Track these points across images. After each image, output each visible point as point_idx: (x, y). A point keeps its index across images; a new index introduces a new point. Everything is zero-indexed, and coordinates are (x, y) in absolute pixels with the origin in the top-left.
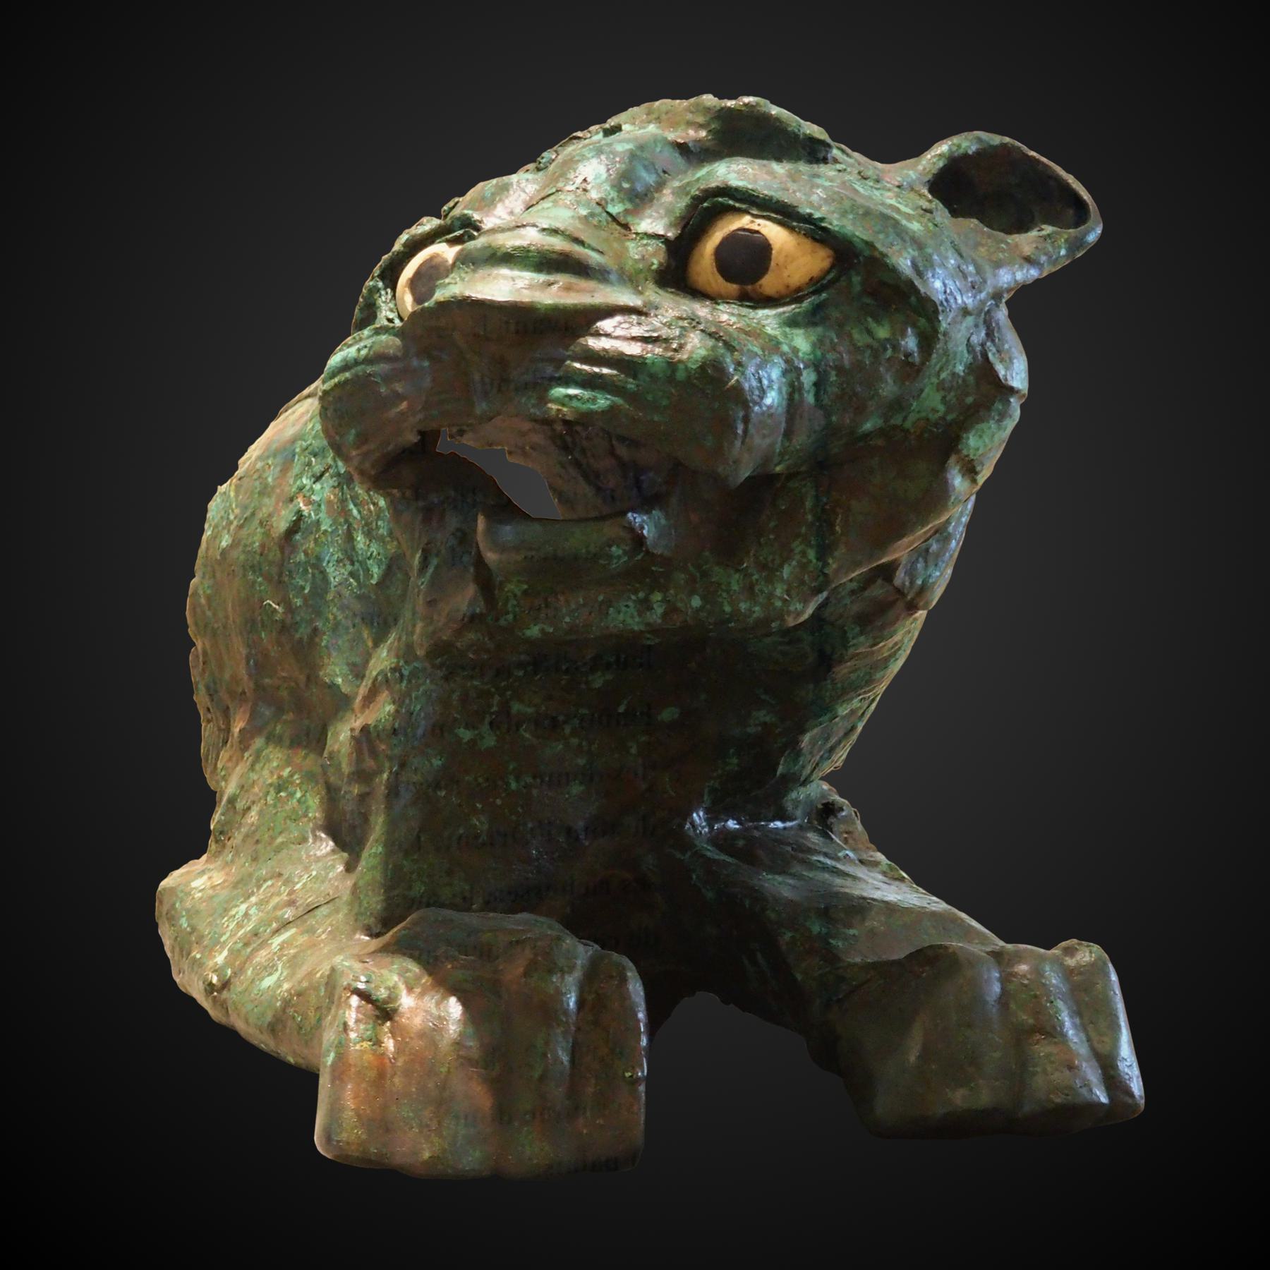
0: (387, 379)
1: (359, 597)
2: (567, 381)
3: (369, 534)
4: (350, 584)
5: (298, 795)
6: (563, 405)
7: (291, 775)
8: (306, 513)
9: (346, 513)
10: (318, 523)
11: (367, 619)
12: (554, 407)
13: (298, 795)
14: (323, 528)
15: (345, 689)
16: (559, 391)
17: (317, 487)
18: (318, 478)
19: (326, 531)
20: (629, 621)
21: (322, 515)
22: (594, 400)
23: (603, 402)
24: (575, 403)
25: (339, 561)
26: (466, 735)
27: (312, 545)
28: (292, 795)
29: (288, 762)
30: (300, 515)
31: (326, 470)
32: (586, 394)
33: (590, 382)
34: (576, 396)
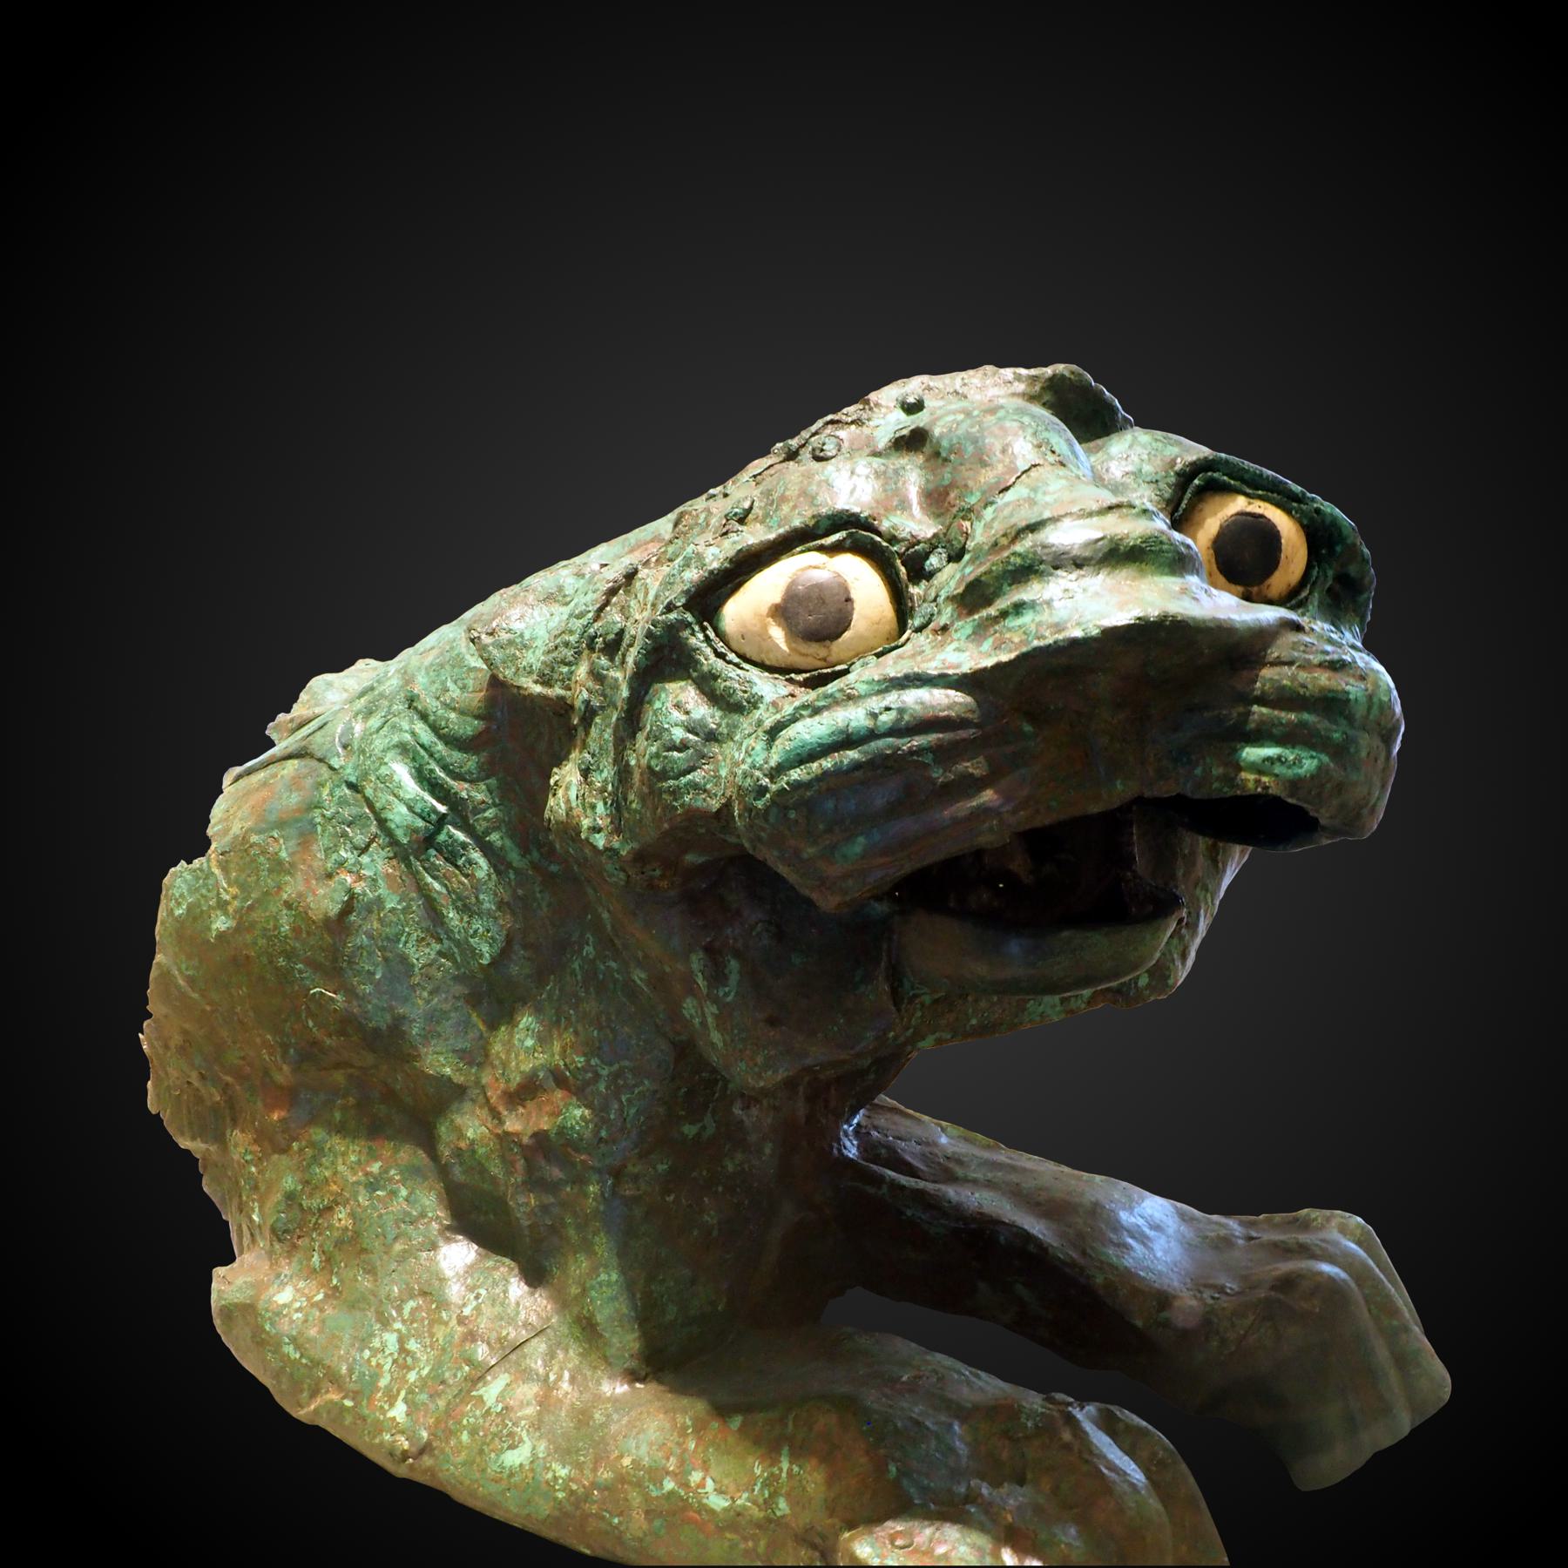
0: (943, 754)
1: (456, 978)
2: (1259, 736)
3: (466, 909)
4: (443, 965)
5: (404, 1192)
6: (1261, 772)
7: (384, 1170)
8: (358, 890)
9: (423, 890)
10: (379, 901)
11: (474, 999)
12: (1249, 777)
13: (404, 1192)
14: (389, 906)
15: (459, 1079)
16: (1253, 753)
17: (365, 859)
18: (364, 850)
19: (393, 910)
20: (1049, 1011)
21: (383, 891)
22: (1298, 762)
23: (1309, 763)
24: (1278, 769)
25: (420, 940)
26: (690, 1130)
27: (376, 925)
28: (393, 1194)
29: (373, 1156)
30: (350, 891)
31: (372, 841)
32: (1290, 755)
33: (1287, 738)
34: (1279, 758)
